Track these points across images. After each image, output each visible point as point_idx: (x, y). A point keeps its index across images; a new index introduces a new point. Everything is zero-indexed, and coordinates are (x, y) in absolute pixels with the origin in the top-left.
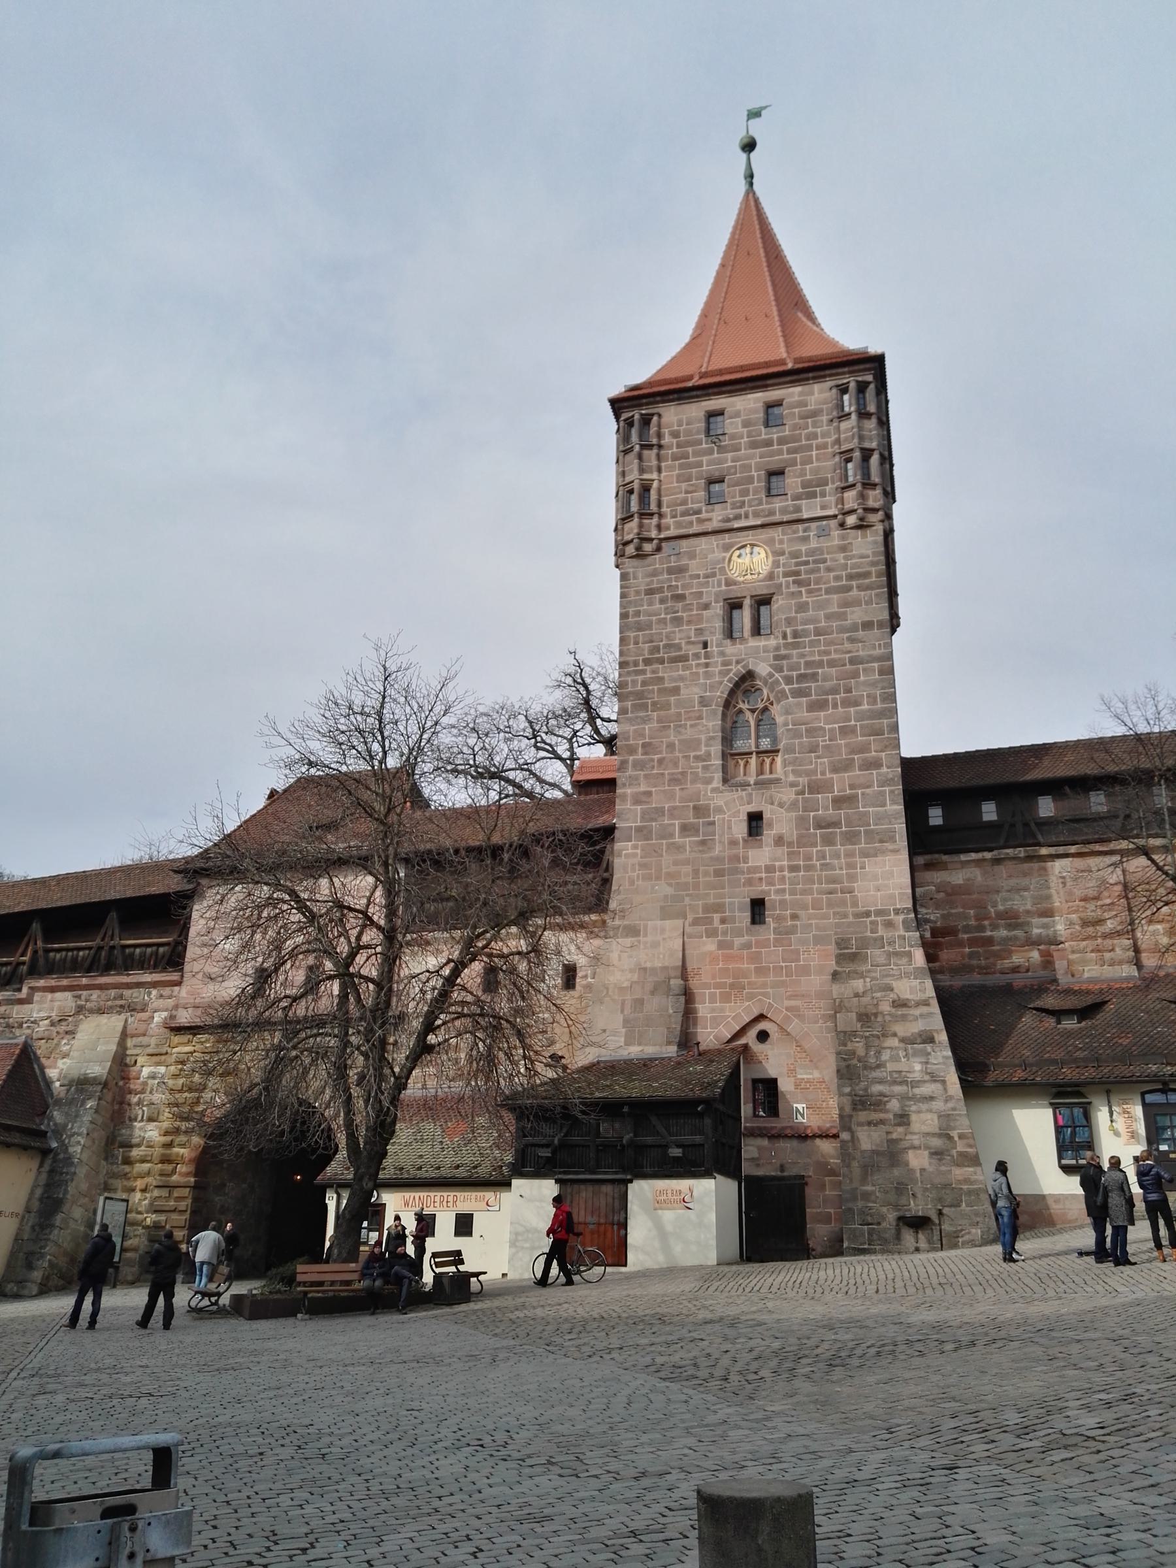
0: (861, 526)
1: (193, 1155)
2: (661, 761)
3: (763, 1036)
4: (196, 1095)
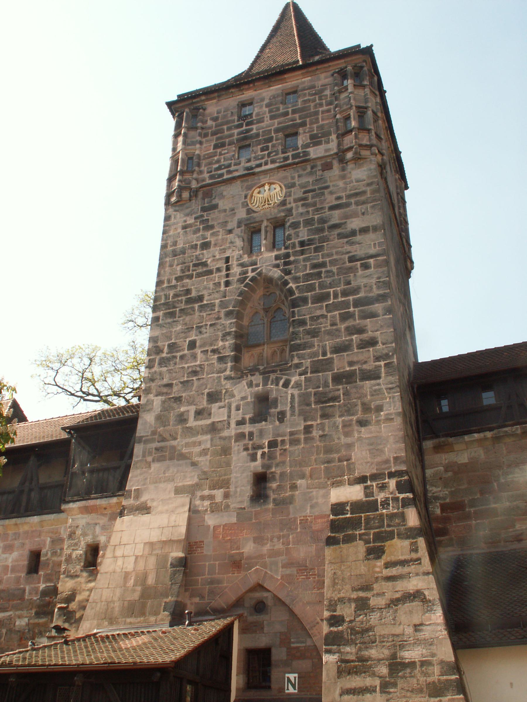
0: (358, 159)
2: (182, 357)
3: (260, 607)
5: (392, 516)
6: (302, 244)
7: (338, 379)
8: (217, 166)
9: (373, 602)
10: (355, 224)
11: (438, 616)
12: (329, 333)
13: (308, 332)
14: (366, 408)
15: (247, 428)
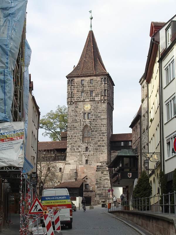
0: (104, 102)
2: (74, 138)
3: (87, 179)
5: (105, 168)
6: (93, 119)
7: (98, 146)
8: (77, 97)
9: (102, 179)
10: (102, 117)
11: (109, 182)
12: (97, 138)
13: (94, 137)
14: (102, 152)
15: (85, 152)
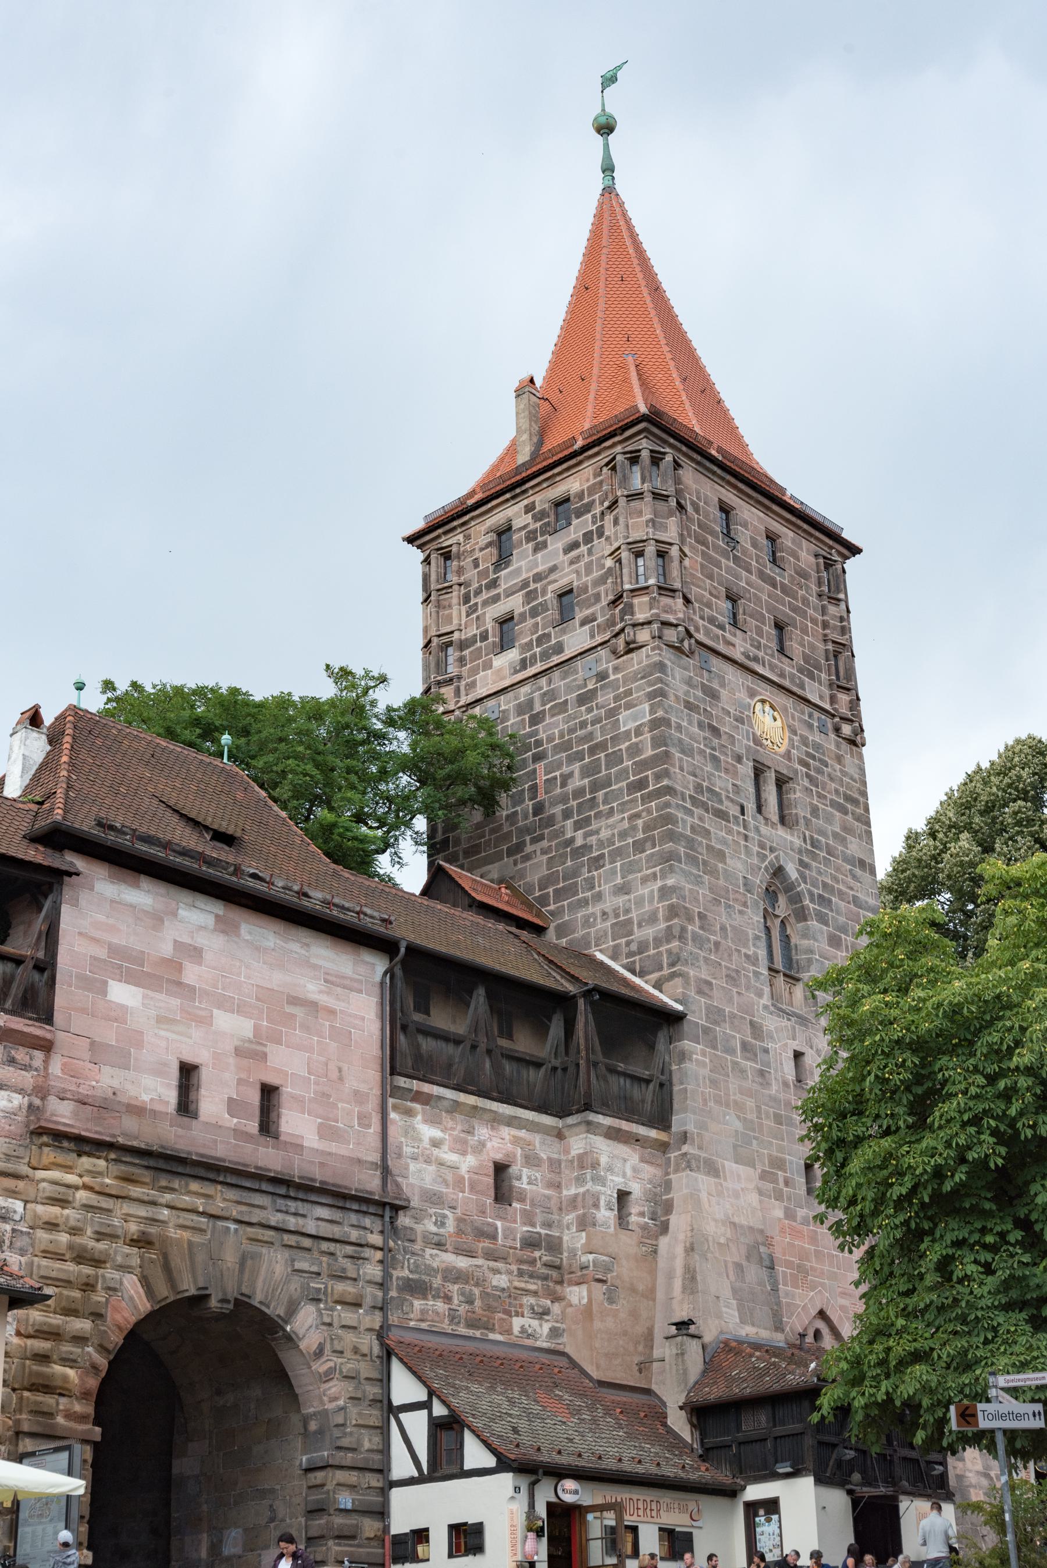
1: (93, 1383)
4: (87, 1270)
